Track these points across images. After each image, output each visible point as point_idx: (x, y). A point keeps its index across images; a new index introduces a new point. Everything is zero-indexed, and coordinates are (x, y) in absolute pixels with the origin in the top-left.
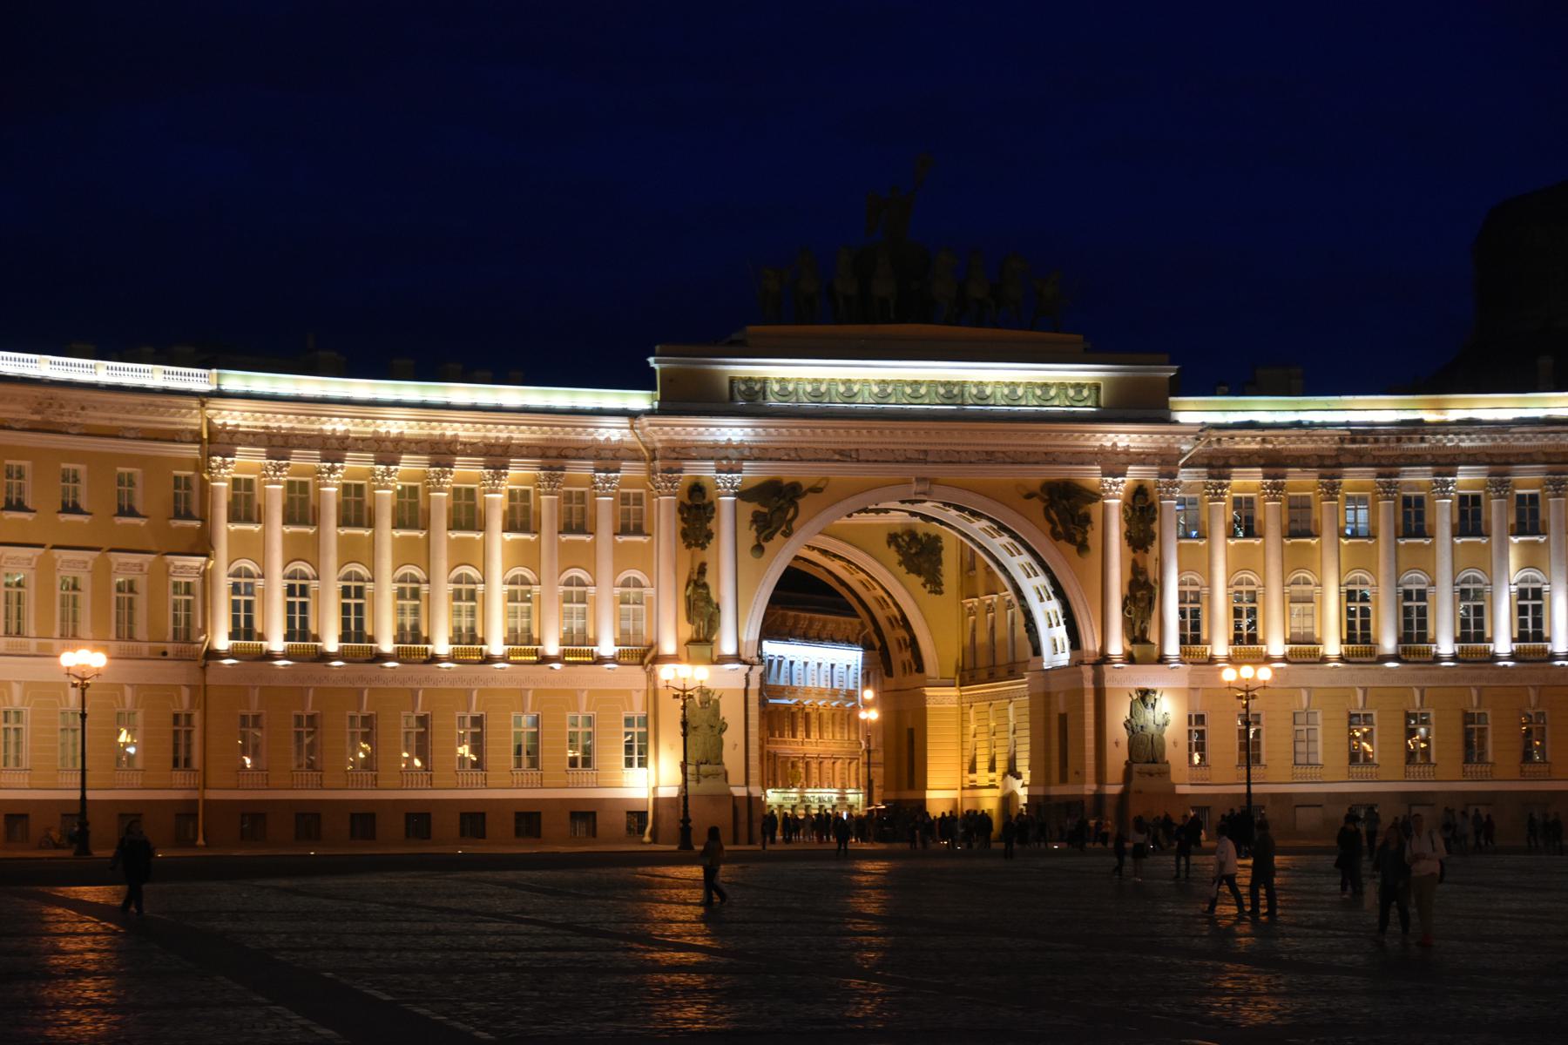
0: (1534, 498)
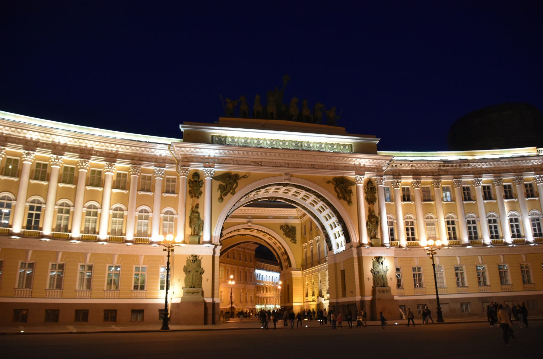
0: (509, 186)
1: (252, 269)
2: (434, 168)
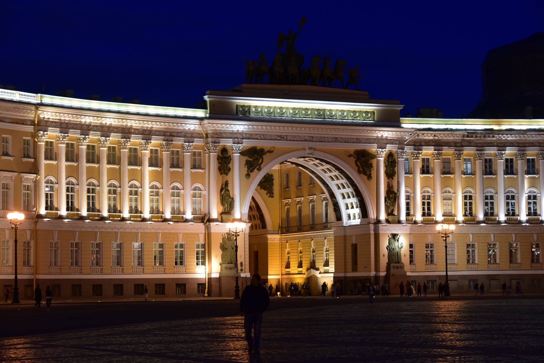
0: (533, 160)
2: (457, 138)
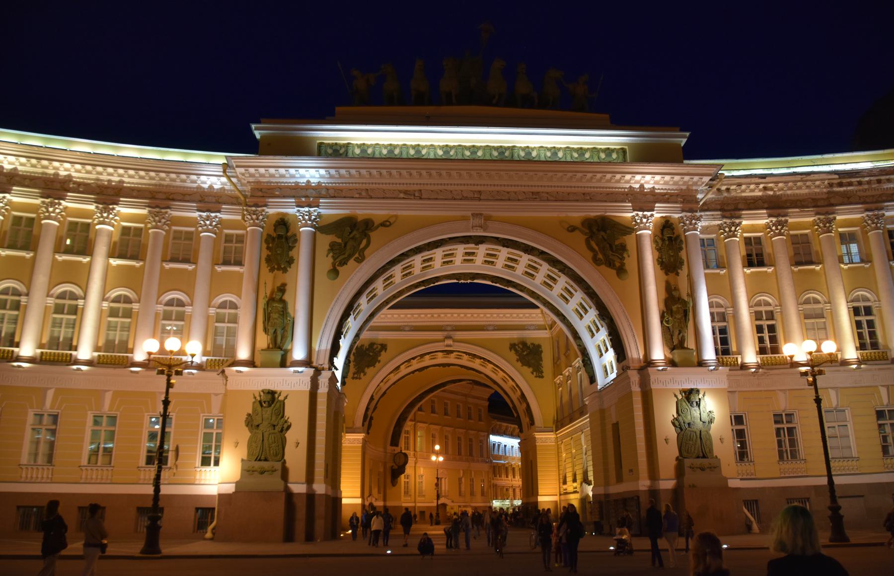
1: (482, 434)
2: (817, 190)
